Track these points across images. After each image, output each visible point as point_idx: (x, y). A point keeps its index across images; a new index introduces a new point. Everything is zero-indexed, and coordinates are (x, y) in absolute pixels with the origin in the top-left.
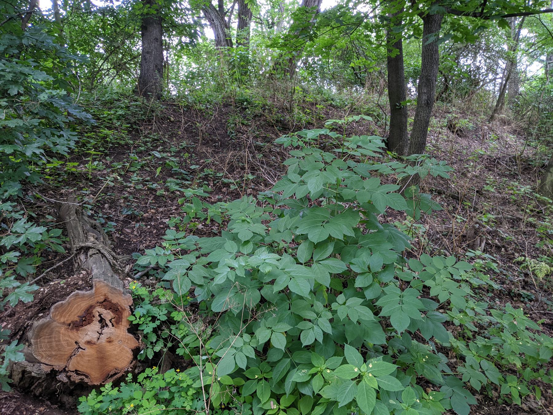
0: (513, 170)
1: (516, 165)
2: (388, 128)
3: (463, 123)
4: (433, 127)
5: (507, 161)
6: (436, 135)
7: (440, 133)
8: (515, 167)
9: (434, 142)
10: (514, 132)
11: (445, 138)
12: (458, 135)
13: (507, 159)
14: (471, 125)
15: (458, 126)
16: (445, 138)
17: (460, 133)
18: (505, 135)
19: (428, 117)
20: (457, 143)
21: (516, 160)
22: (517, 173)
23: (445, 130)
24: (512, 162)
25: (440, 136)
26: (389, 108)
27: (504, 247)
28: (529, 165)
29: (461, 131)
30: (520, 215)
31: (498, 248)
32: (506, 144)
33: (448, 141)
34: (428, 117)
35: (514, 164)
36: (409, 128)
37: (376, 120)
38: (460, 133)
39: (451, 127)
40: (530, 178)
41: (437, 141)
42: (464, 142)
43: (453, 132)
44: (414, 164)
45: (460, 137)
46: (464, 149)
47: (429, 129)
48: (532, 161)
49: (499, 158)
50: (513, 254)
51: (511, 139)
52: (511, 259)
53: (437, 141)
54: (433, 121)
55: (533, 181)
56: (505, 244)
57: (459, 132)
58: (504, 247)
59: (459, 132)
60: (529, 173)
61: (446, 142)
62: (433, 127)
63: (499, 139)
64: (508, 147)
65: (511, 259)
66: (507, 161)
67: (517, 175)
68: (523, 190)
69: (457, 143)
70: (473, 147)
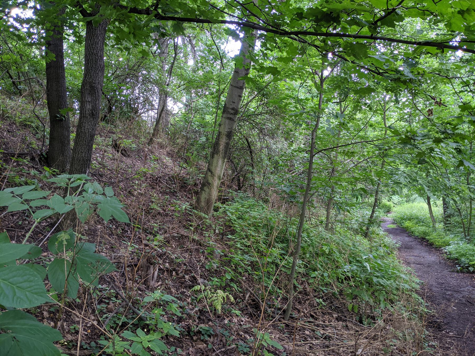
0: (172, 188)
1: (175, 184)
2: (47, 142)
3: (126, 143)
4: (98, 145)
5: (167, 180)
6: (101, 153)
7: (105, 151)
8: (174, 185)
9: (99, 159)
10: (169, 154)
11: (111, 156)
12: (122, 154)
13: (167, 178)
14: (134, 145)
15: (122, 145)
16: (111, 156)
17: (125, 152)
18: (163, 157)
19: (93, 129)
20: (122, 162)
21: (174, 179)
22: (176, 190)
23: (110, 149)
24: (171, 180)
25: (105, 154)
26: (48, 118)
27: (174, 270)
28: (185, 183)
29: (125, 151)
30: (184, 232)
31: (170, 272)
32: (164, 165)
33: (114, 159)
34: (93, 129)
35: (173, 182)
36: (72, 143)
37: (34, 132)
38: (125, 152)
39: (116, 146)
40: (186, 195)
41: (103, 158)
42: (129, 161)
43: (118, 151)
44: (65, 191)
45: (125, 156)
46: (129, 168)
47: (94, 146)
48: (187, 180)
49: (160, 177)
50: (184, 277)
51: (168, 160)
52: (182, 283)
53: (103, 158)
54: (98, 139)
55: (188, 198)
56: (175, 266)
57: (124, 152)
58: (174, 270)
59: (124, 152)
60: (185, 191)
61: (111, 160)
62: (98, 145)
63: (157, 160)
64: (166, 167)
65: (182, 283)
66: (167, 180)
67: (176, 192)
68: (184, 207)
69: (122, 162)
70: (136, 166)
